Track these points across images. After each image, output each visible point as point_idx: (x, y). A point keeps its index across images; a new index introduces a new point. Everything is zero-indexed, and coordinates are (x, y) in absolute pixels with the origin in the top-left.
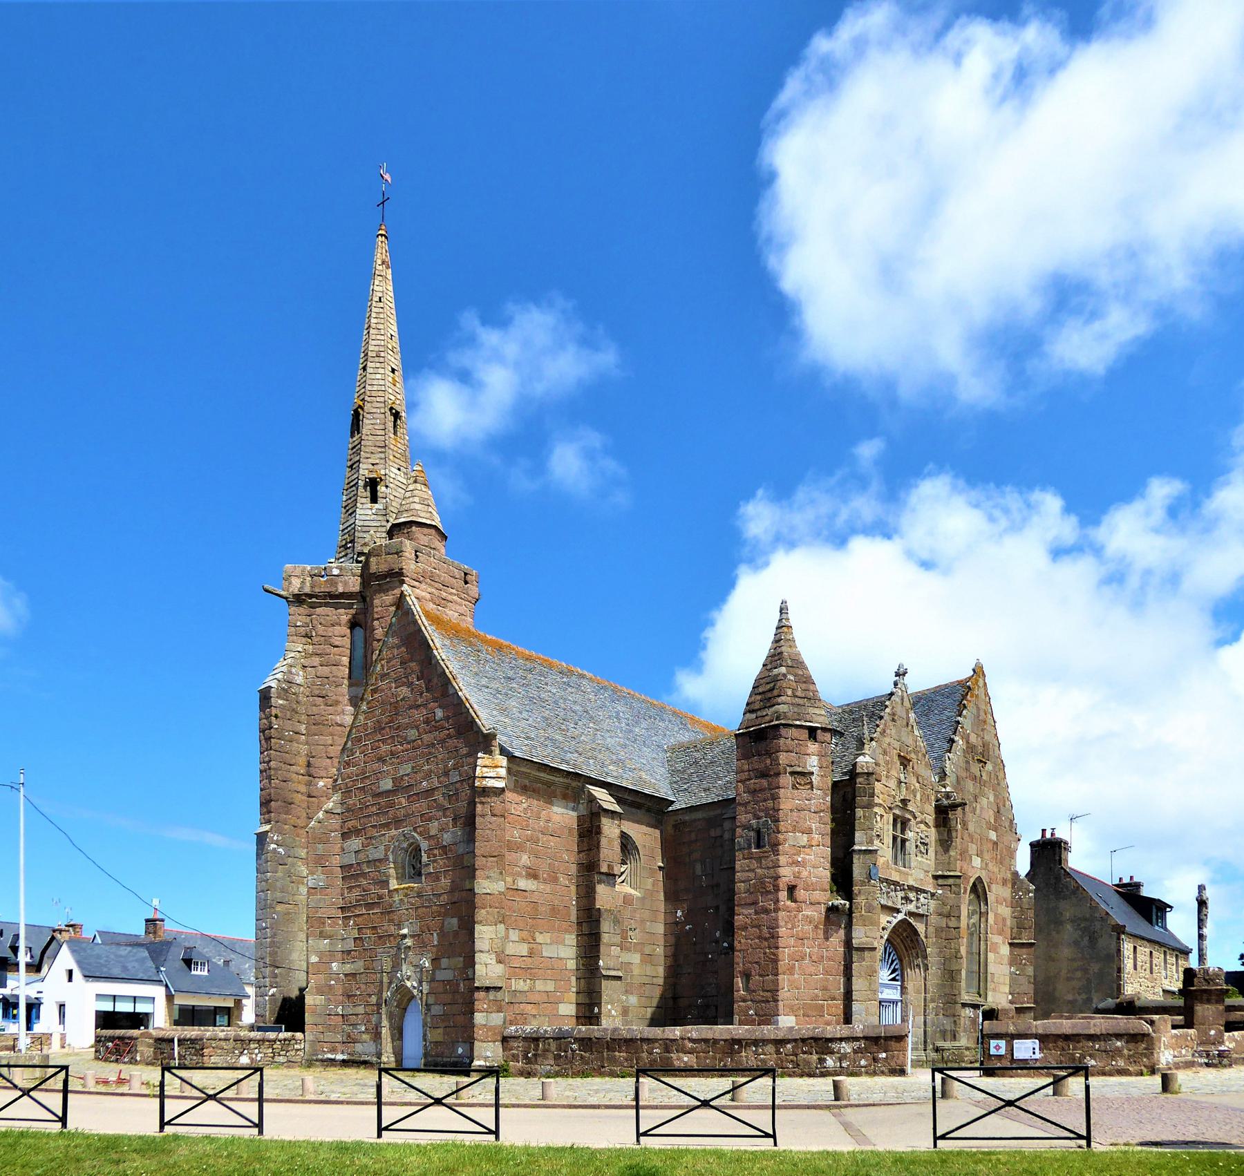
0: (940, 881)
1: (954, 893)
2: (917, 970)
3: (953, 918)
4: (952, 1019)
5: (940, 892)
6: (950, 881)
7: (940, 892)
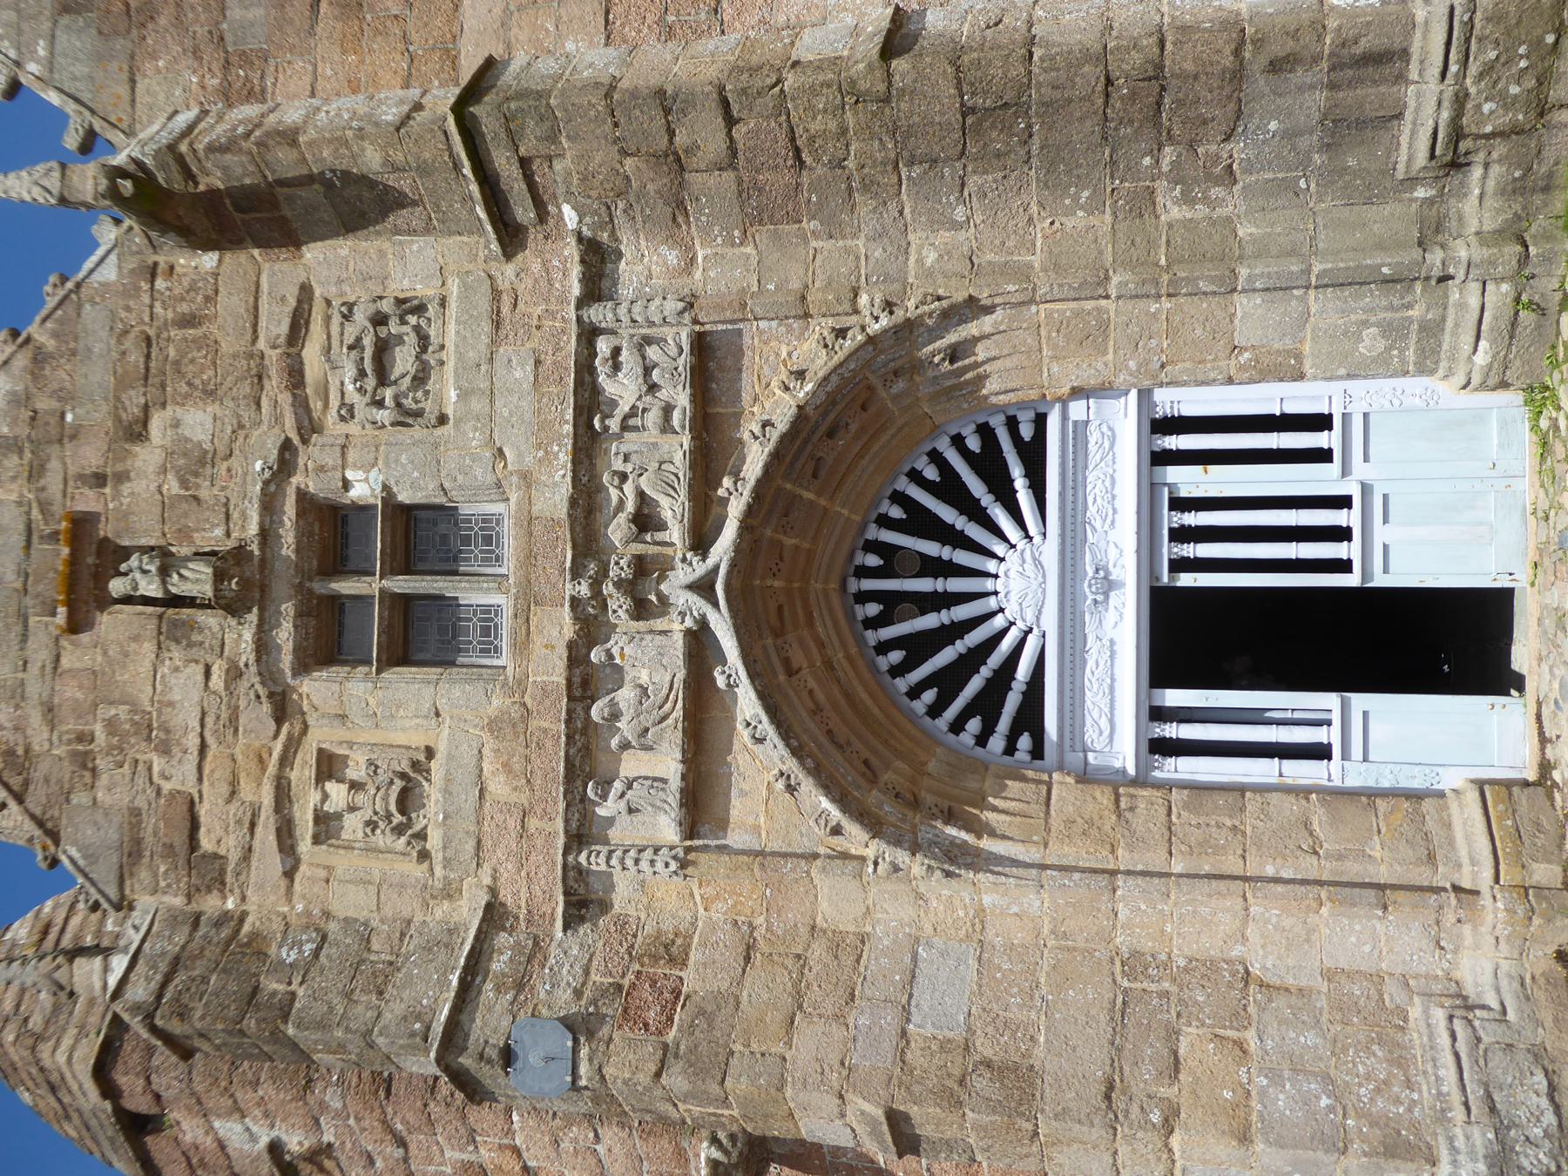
0: (523, 212)
1: (552, 137)
2: (981, 352)
3: (681, 139)
4: (1260, 82)
5: (569, 215)
6: (503, 163)
7: (569, 215)
